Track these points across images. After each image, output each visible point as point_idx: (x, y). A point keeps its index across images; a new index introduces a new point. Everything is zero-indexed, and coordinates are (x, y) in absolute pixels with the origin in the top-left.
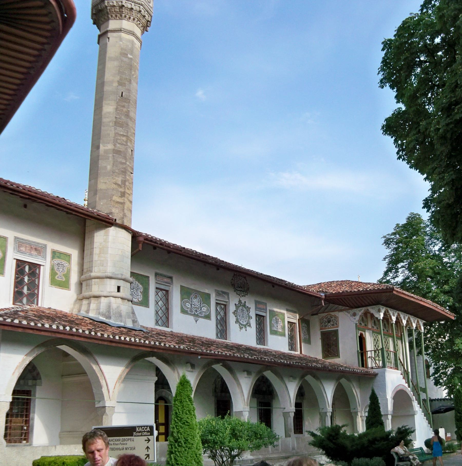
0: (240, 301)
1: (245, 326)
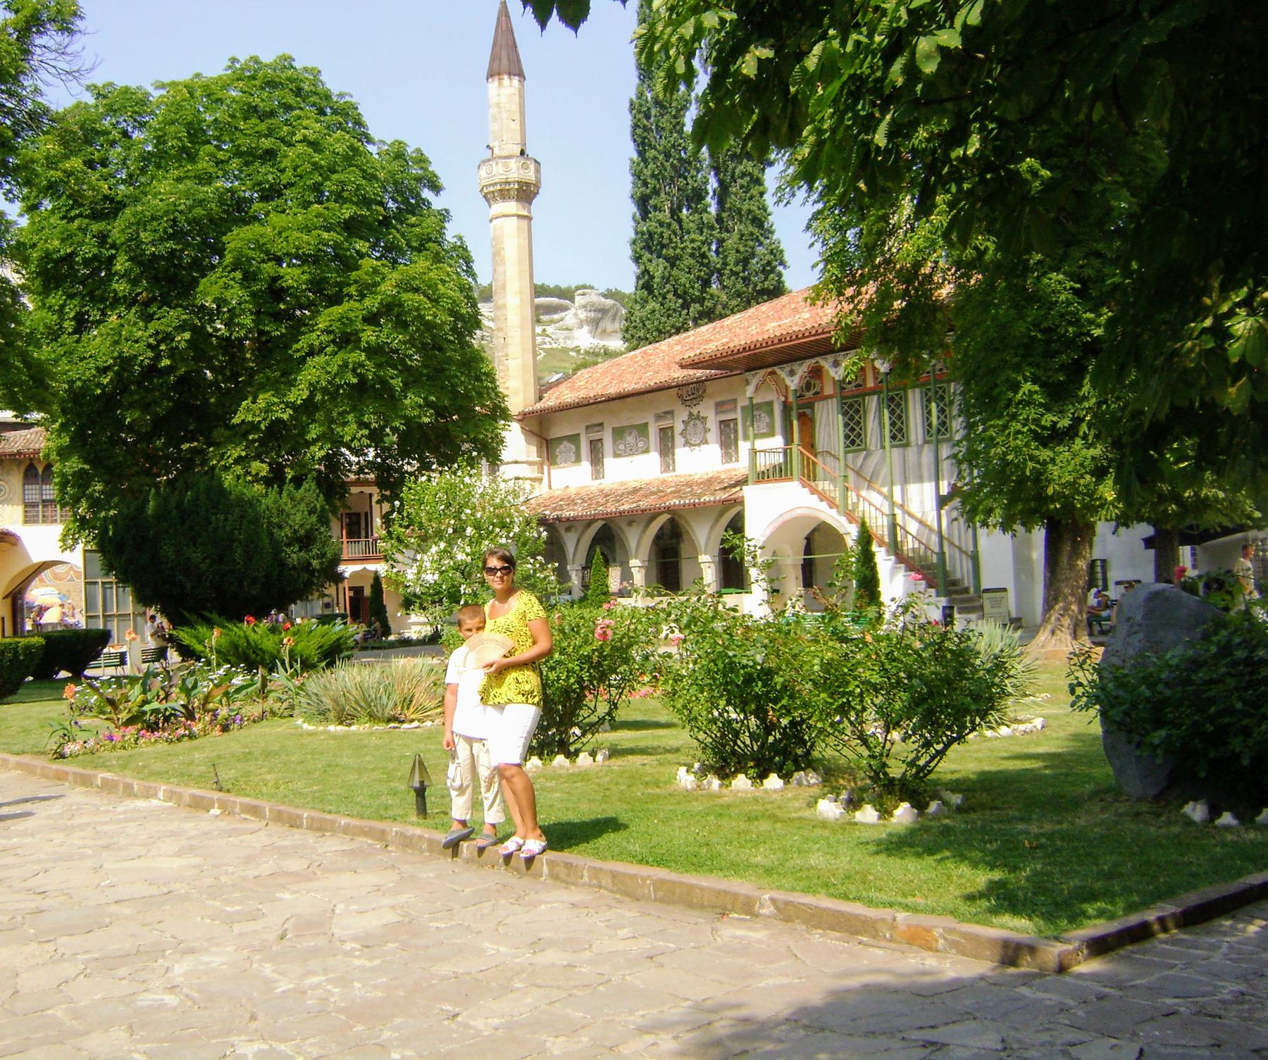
0: (691, 414)
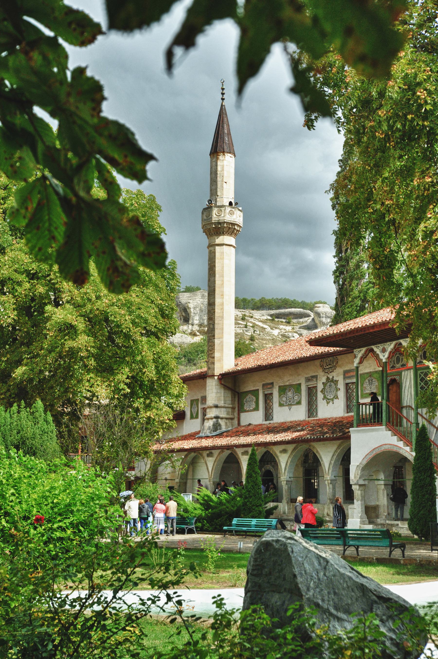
0: (328, 378)
1: (332, 400)
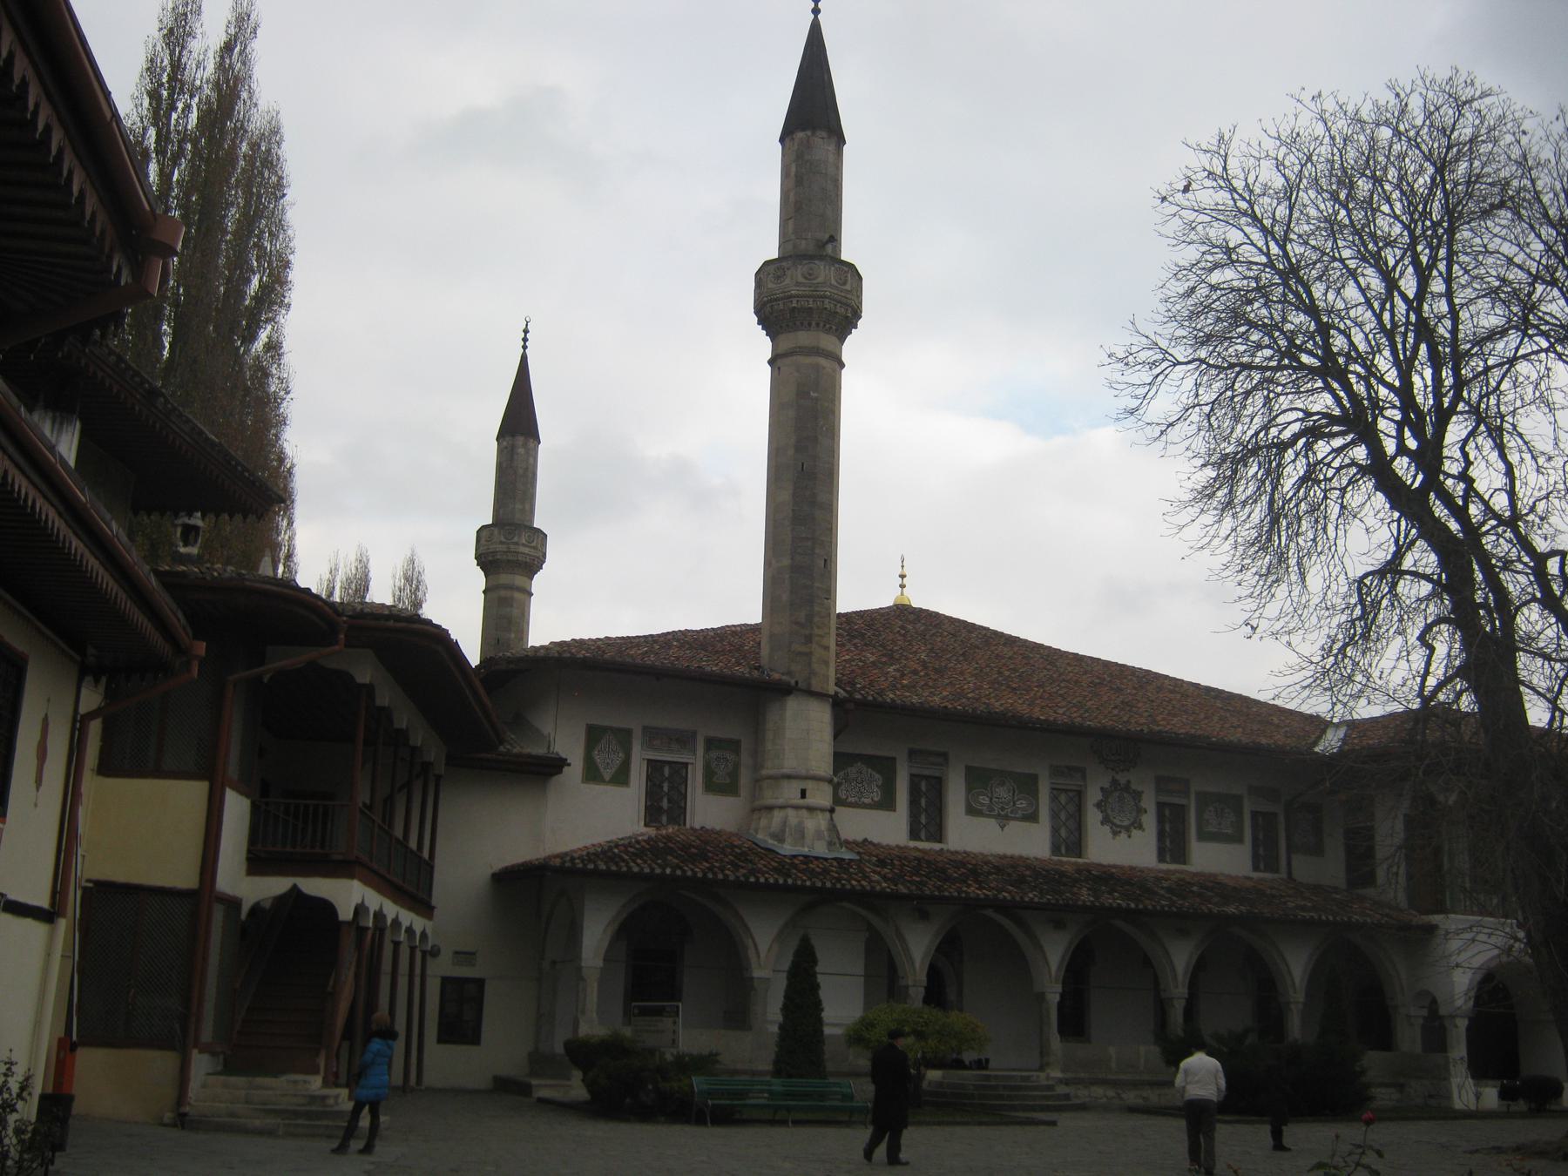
0: (1114, 782)
1: (1128, 829)
